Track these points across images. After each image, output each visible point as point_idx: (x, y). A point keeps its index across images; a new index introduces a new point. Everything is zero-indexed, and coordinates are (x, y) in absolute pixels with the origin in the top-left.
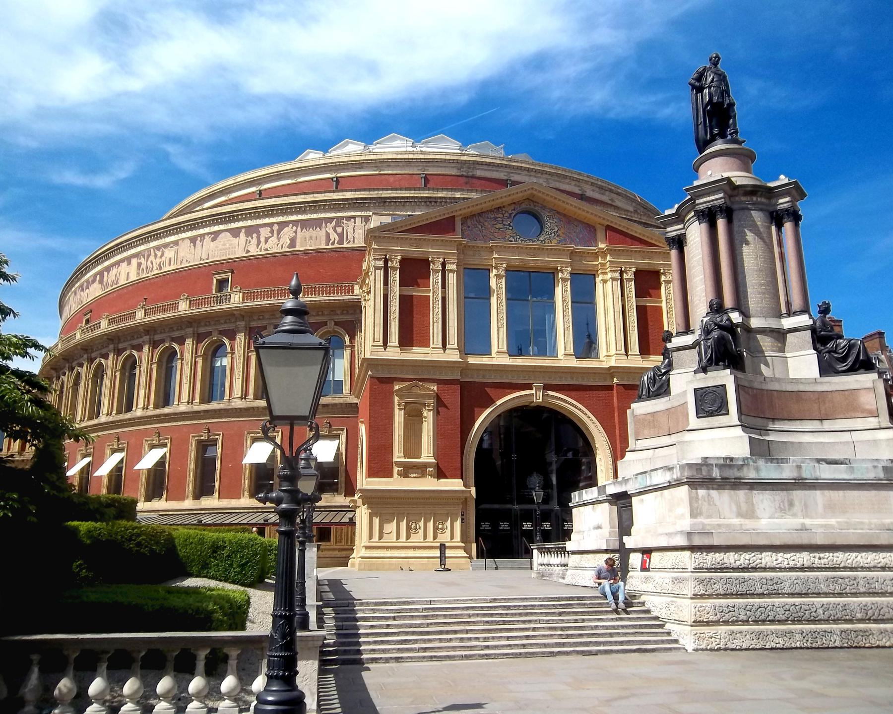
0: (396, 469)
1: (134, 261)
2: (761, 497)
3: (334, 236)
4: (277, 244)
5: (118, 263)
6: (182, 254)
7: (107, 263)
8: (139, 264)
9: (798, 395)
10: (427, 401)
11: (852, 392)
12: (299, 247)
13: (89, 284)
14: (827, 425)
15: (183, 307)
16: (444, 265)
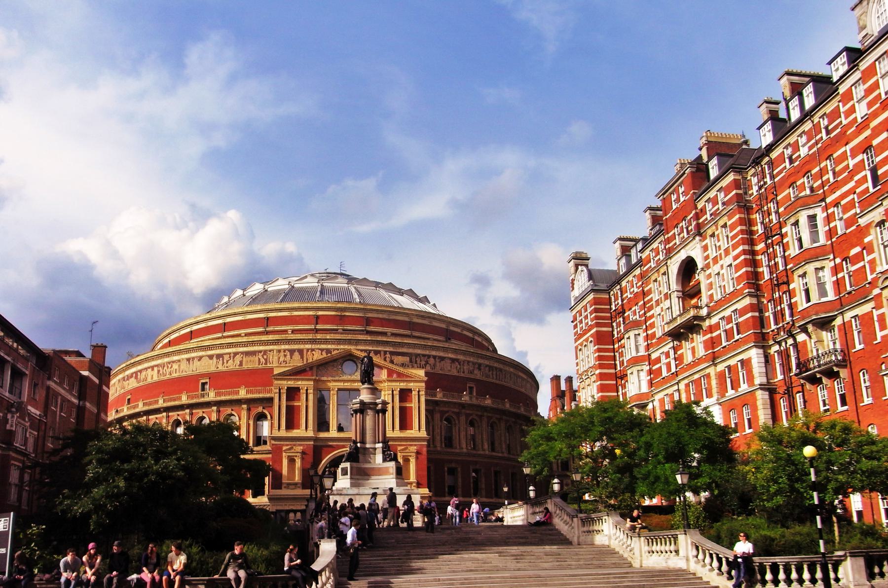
0: (283, 486)
1: (156, 369)
3: (262, 360)
4: (232, 365)
5: (146, 369)
6: (182, 367)
7: (139, 368)
8: (159, 371)
9: (380, 468)
11: (387, 468)
12: (245, 367)
15: (184, 399)
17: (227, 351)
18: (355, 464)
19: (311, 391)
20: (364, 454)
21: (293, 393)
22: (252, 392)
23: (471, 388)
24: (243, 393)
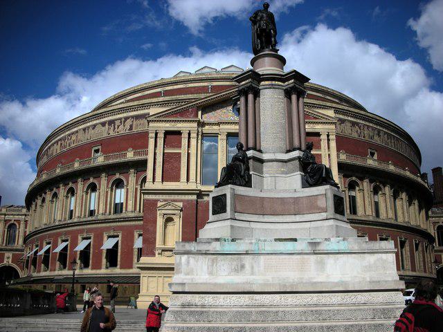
0: (157, 253)
1: (59, 142)
2: (223, 262)
4: (123, 130)
5: (53, 145)
8: (61, 144)
10: (176, 211)
13: (43, 155)
14: (298, 218)
15: (77, 166)
16: (189, 134)
17: (118, 116)
18: (241, 190)
19: (193, 135)
20: (260, 171)
21: (172, 136)
22: (139, 154)
23: (372, 154)
24: (130, 156)
